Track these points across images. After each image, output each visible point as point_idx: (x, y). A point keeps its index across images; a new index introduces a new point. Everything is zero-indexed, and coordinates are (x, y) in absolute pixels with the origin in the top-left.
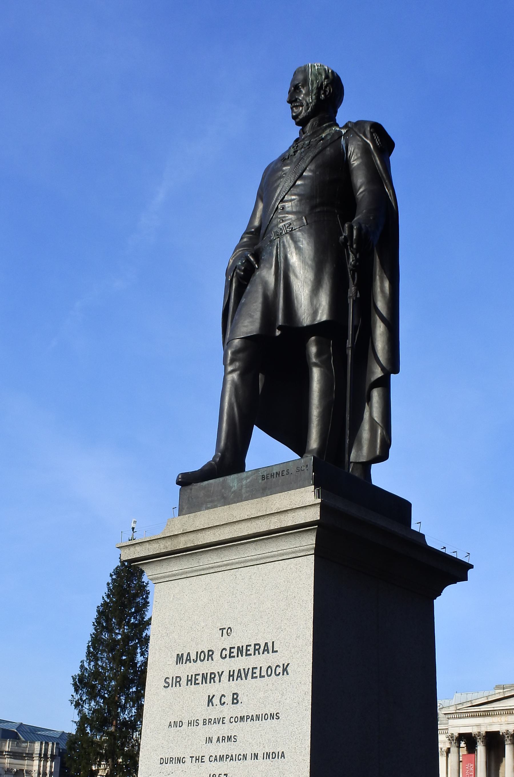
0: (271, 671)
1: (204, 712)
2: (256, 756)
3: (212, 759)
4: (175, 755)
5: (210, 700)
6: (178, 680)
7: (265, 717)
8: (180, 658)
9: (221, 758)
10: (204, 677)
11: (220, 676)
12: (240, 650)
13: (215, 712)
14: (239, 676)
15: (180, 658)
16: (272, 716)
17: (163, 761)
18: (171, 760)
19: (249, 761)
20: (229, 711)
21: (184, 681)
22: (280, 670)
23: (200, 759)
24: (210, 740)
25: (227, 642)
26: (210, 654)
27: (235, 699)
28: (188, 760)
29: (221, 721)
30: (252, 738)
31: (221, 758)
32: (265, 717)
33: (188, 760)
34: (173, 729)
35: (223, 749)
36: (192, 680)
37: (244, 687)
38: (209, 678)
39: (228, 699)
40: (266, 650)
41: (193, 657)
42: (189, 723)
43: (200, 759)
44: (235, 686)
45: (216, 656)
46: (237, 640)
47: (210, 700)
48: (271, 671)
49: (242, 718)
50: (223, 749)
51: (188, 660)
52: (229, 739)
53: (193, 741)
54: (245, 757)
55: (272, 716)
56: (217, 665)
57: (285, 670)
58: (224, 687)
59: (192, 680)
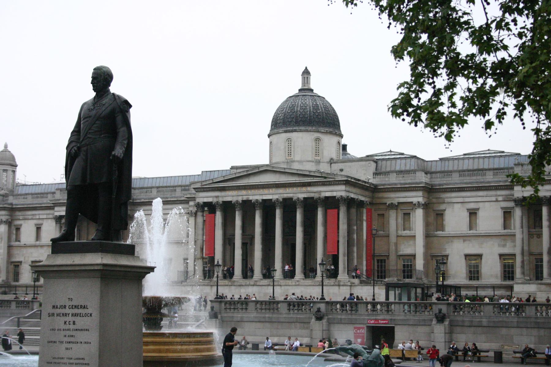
0: (86, 315)
1: (63, 327)
2: (81, 343)
4: (53, 340)
5: (65, 323)
6: (53, 314)
7: (84, 330)
8: (54, 307)
9: (70, 342)
10: (63, 314)
11: (69, 314)
12: (75, 306)
13: (67, 327)
14: (75, 315)
15: (54, 307)
16: (87, 330)
17: (49, 342)
18: (52, 342)
19: (79, 344)
20: (72, 327)
21: (55, 315)
22: (89, 315)
23: (62, 342)
24: (65, 336)
25: (71, 303)
26: (65, 307)
27: (74, 323)
28: (58, 342)
31: (70, 342)
32: (84, 330)
33: (58, 342)
34: (52, 332)
37: (77, 319)
38: (65, 315)
39: (72, 323)
40: (84, 307)
41: (59, 307)
42: (58, 330)
43: (62, 342)
44: (74, 319)
45: (67, 307)
46: (74, 303)
47: (65, 323)
48: (86, 315)
49: (76, 330)
51: (57, 307)
52: (72, 336)
54: (78, 343)
55: (87, 330)
56: (67, 311)
57: (91, 315)
58: (70, 318)
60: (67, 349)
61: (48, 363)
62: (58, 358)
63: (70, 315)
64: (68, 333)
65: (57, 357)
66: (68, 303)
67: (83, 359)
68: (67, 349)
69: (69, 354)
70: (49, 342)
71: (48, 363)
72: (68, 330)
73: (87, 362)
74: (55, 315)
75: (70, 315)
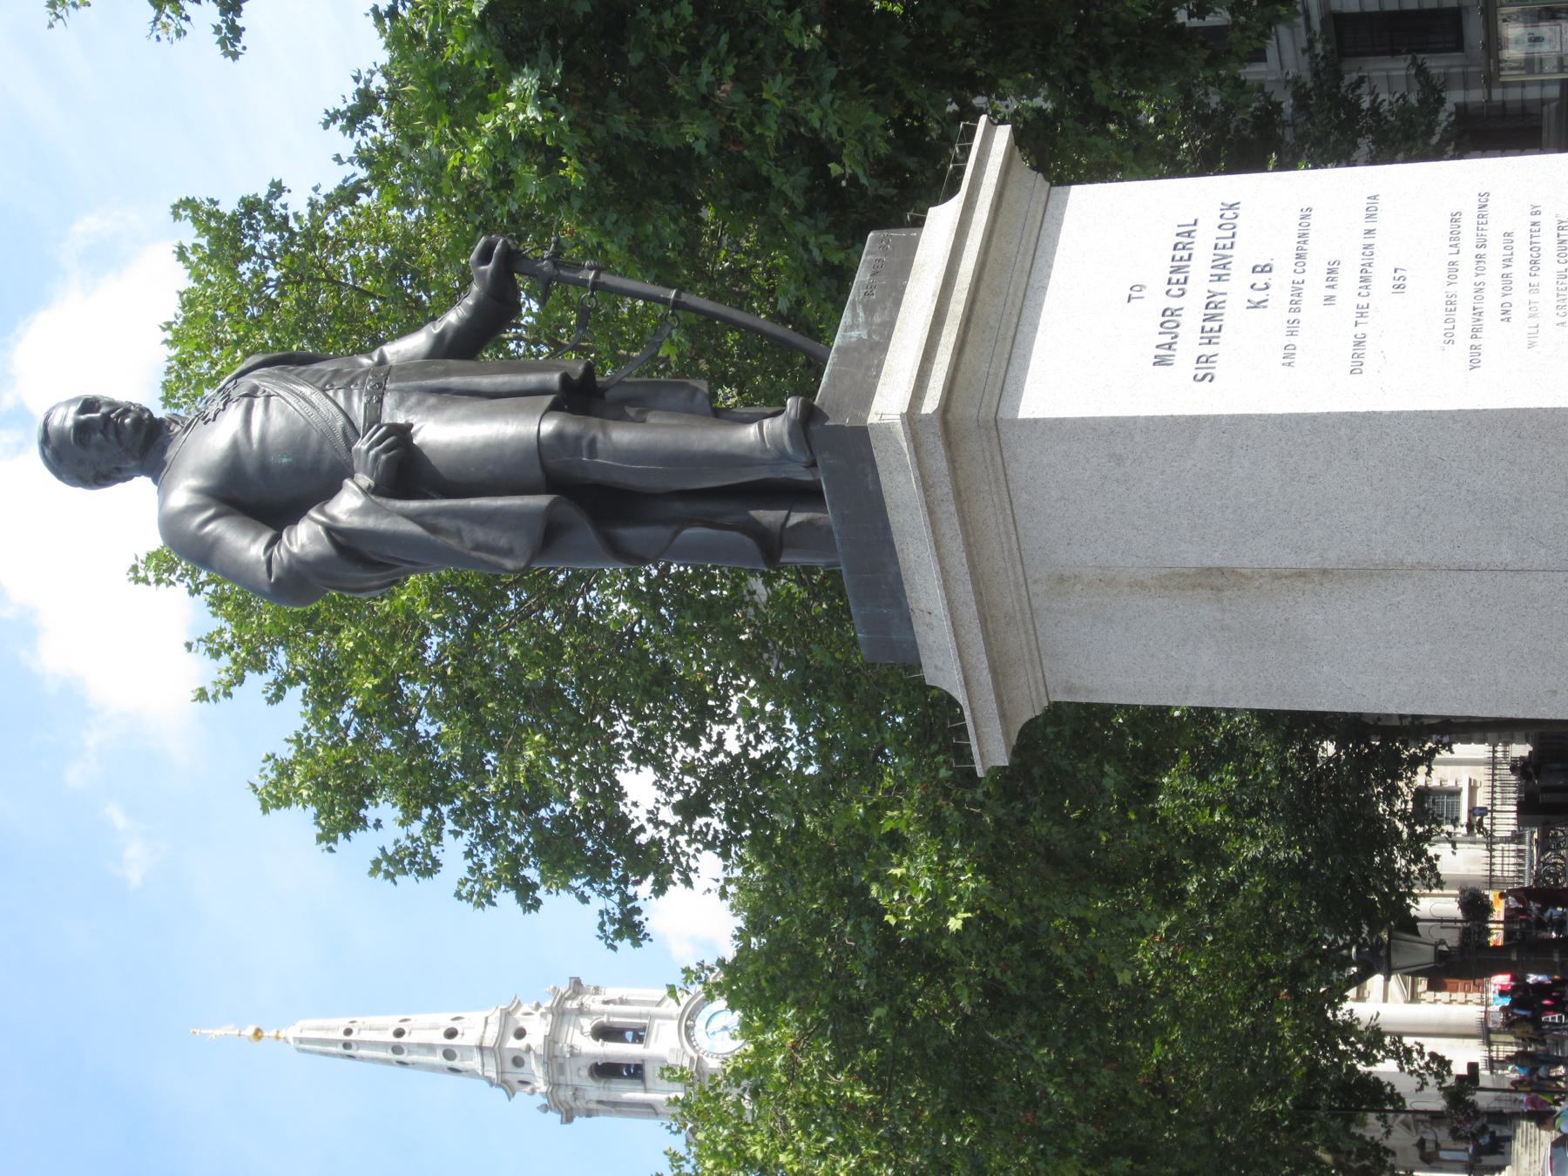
3: (1364, 292)
13: (1280, 296)
19: (1377, 241)
23: (1362, 312)
27: (1266, 269)
29: (1297, 290)
35: (1349, 279)
38: (1213, 310)
39: (1260, 279)
41: (1167, 339)
43: (1362, 312)
50: (1349, 279)
53: (1328, 331)
60: (1399, 288)
61: (1474, 364)
66: (1155, 299)
67: (1455, 219)
68: (1399, 288)
71: (1474, 364)
72: (1297, 290)
73: (1475, 203)
75: (1217, 287)
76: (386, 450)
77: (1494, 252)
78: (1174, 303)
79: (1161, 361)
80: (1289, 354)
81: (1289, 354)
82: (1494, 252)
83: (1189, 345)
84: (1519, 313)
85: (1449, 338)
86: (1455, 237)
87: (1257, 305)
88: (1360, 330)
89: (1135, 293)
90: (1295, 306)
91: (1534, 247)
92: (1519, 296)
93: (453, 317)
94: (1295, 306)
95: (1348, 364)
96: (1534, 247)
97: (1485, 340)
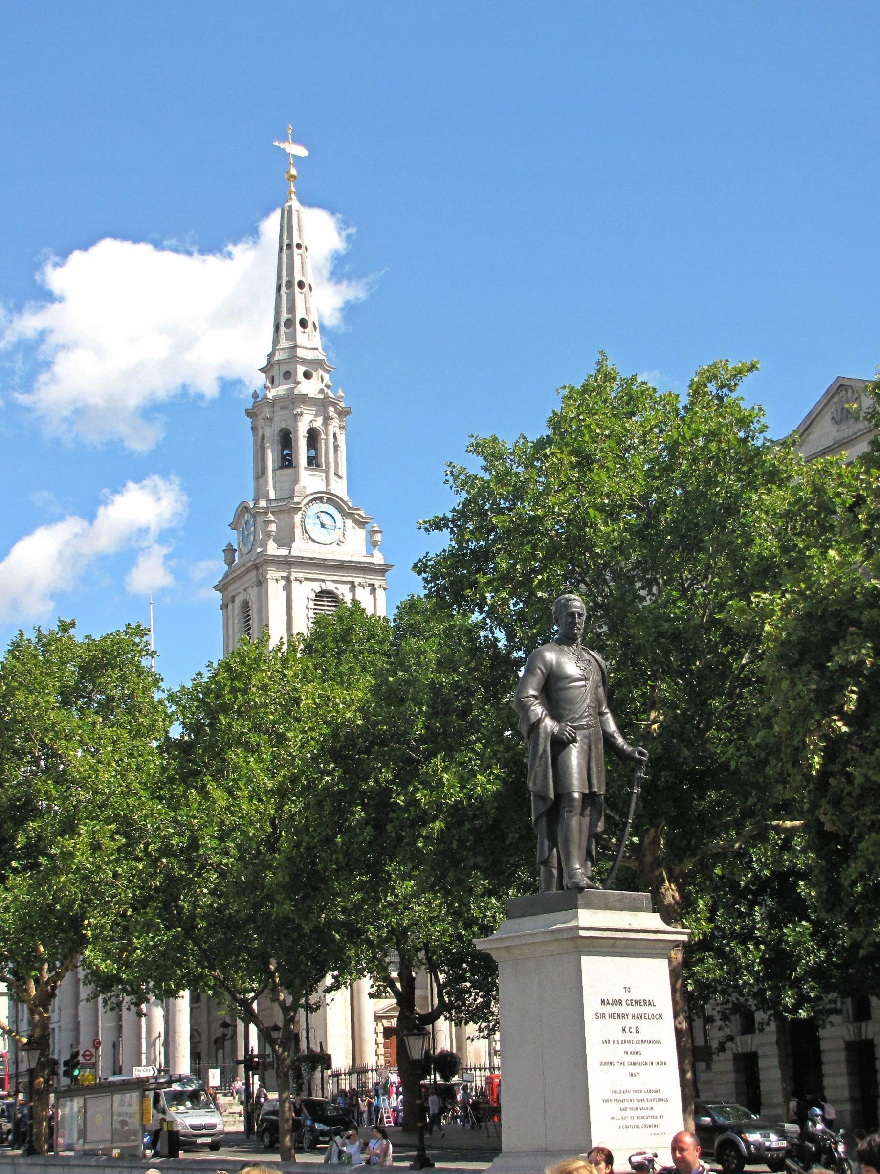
0: (654, 1017)
1: (622, 1037)
13: (627, 1036)
15: (603, 1002)
17: (602, 1064)
20: (634, 1037)
22: (658, 1017)
23: (622, 1064)
25: (629, 996)
27: (637, 1031)
30: (649, 1053)
36: (612, 1016)
39: (633, 1030)
41: (611, 1002)
43: (622, 1064)
47: (624, 1030)
48: (654, 1017)
52: (637, 1053)
53: (616, 1053)
58: (630, 1023)
59: (612, 1016)
61: (605, 1101)
62: (620, 1092)
63: (630, 1016)
64: (630, 1048)
65: (618, 1089)
69: (633, 1084)
70: (602, 1064)
71: (605, 1101)
72: (629, 1042)
74: (607, 1016)
75: (630, 1016)
76: (567, 738)
77: (645, 1105)
78: (624, 1003)
79: (603, 1002)
80: (606, 1042)
81: (606, 1042)
82: (645, 1105)
83: (608, 1009)
84: (624, 1114)
85: (614, 1092)
86: (651, 1091)
87: (624, 1030)
88: (616, 1064)
89: (628, 989)
90: (624, 1042)
91: (648, 1117)
92: (629, 1113)
93: (620, 740)
94: (624, 1042)
95: (604, 1061)
96: (648, 1117)
97: (614, 1104)
